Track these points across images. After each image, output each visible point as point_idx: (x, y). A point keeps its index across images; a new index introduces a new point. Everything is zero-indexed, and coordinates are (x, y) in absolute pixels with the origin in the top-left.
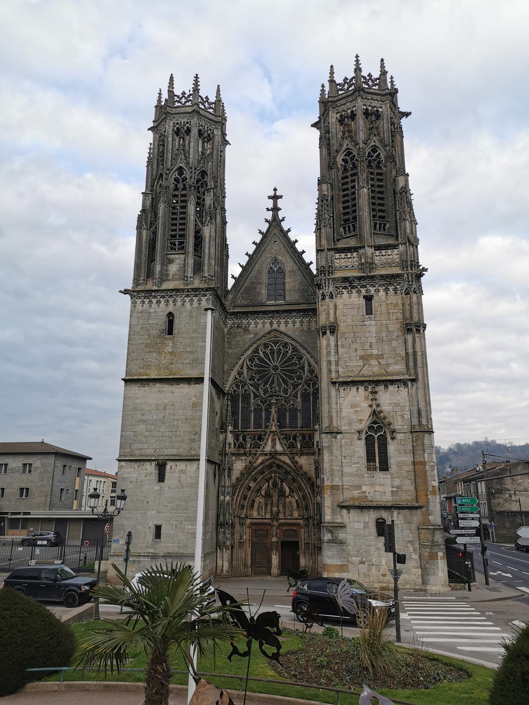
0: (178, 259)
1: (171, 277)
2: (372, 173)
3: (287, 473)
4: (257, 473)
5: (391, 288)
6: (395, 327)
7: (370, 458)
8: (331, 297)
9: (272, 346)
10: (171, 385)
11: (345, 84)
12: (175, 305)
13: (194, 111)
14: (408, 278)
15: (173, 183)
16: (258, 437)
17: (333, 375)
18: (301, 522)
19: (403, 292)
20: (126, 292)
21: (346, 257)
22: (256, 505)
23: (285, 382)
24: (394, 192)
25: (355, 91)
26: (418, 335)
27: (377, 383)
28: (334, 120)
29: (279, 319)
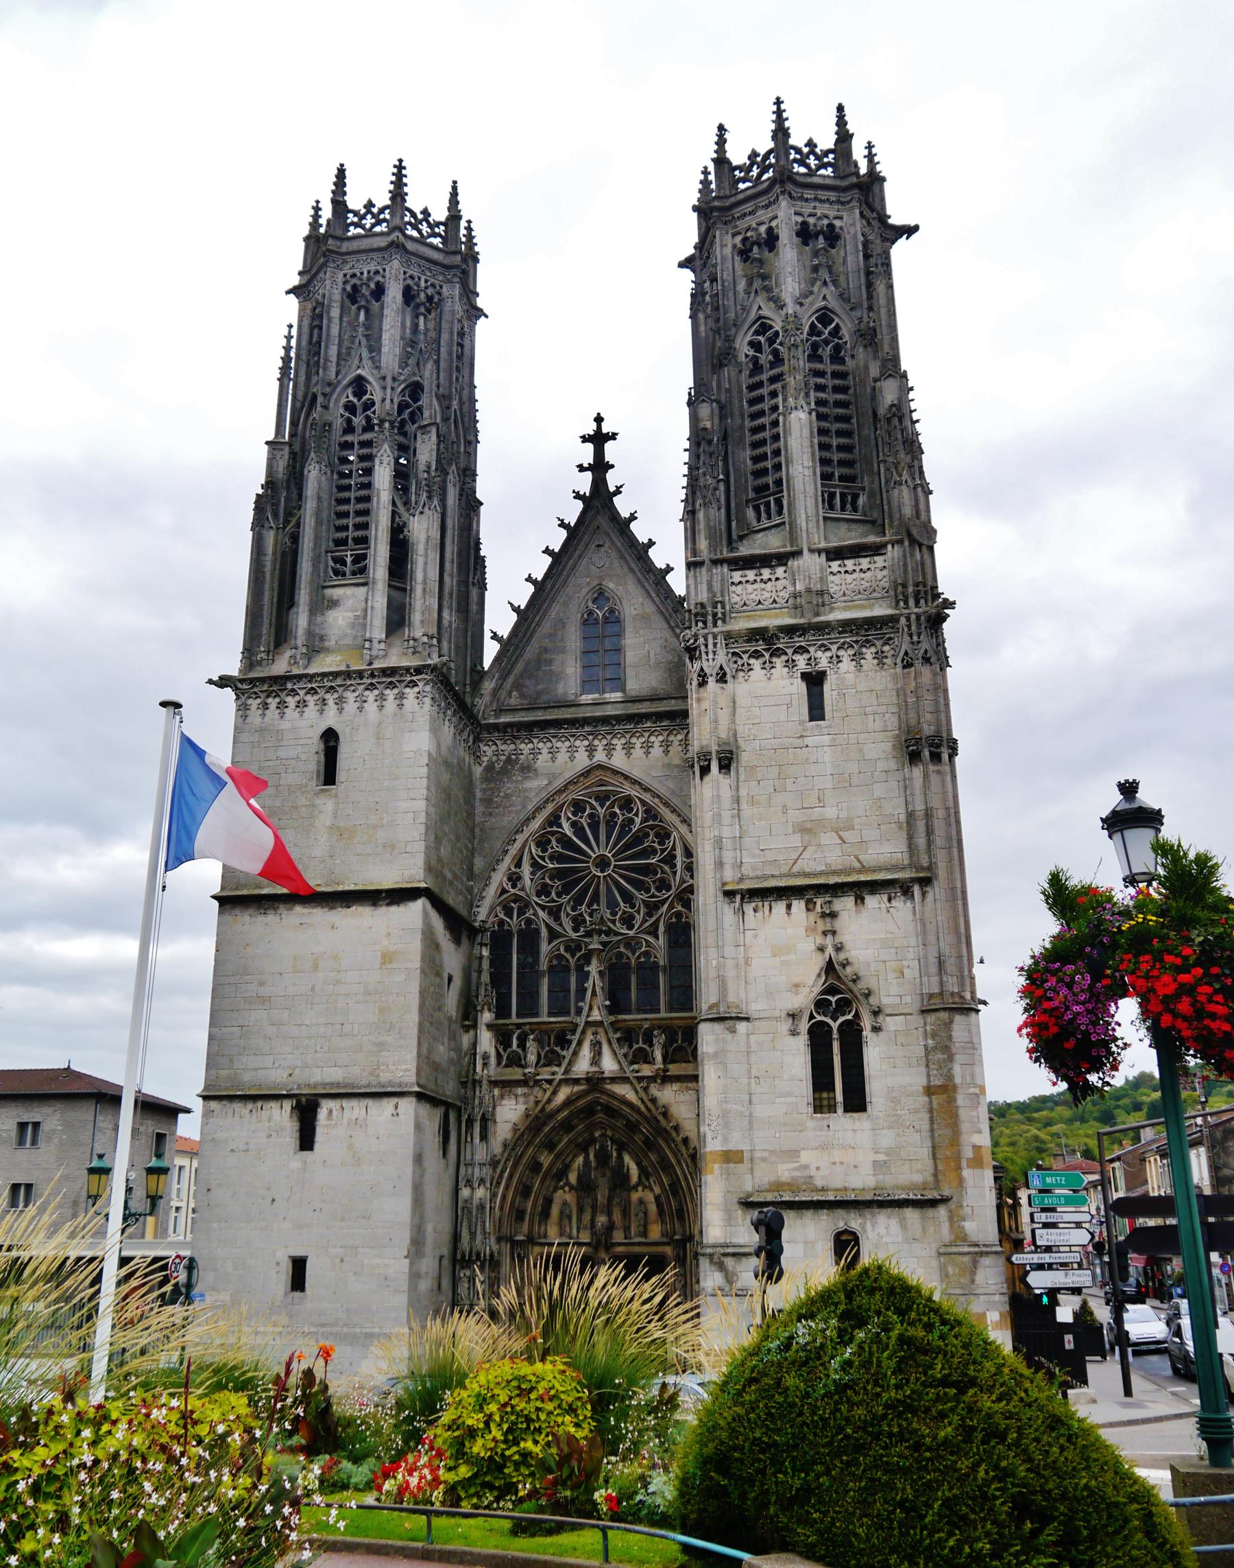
0: (350, 597)
1: (333, 643)
2: (821, 374)
3: (632, 1127)
4: (553, 1129)
5: (869, 653)
6: (879, 748)
8: (722, 678)
9: (593, 807)
10: (332, 908)
11: (752, 165)
12: (341, 710)
13: (392, 244)
14: (909, 626)
15: (342, 416)
16: (557, 1037)
18: (668, 1250)
19: (899, 661)
20: (223, 682)
21: (758, 579)
22: (555, 1211)
23: (628, 898)
24: (875, 414)
25: (773, 182)
26: (936, 768)
28: (728, 251)
29: (609, 737)
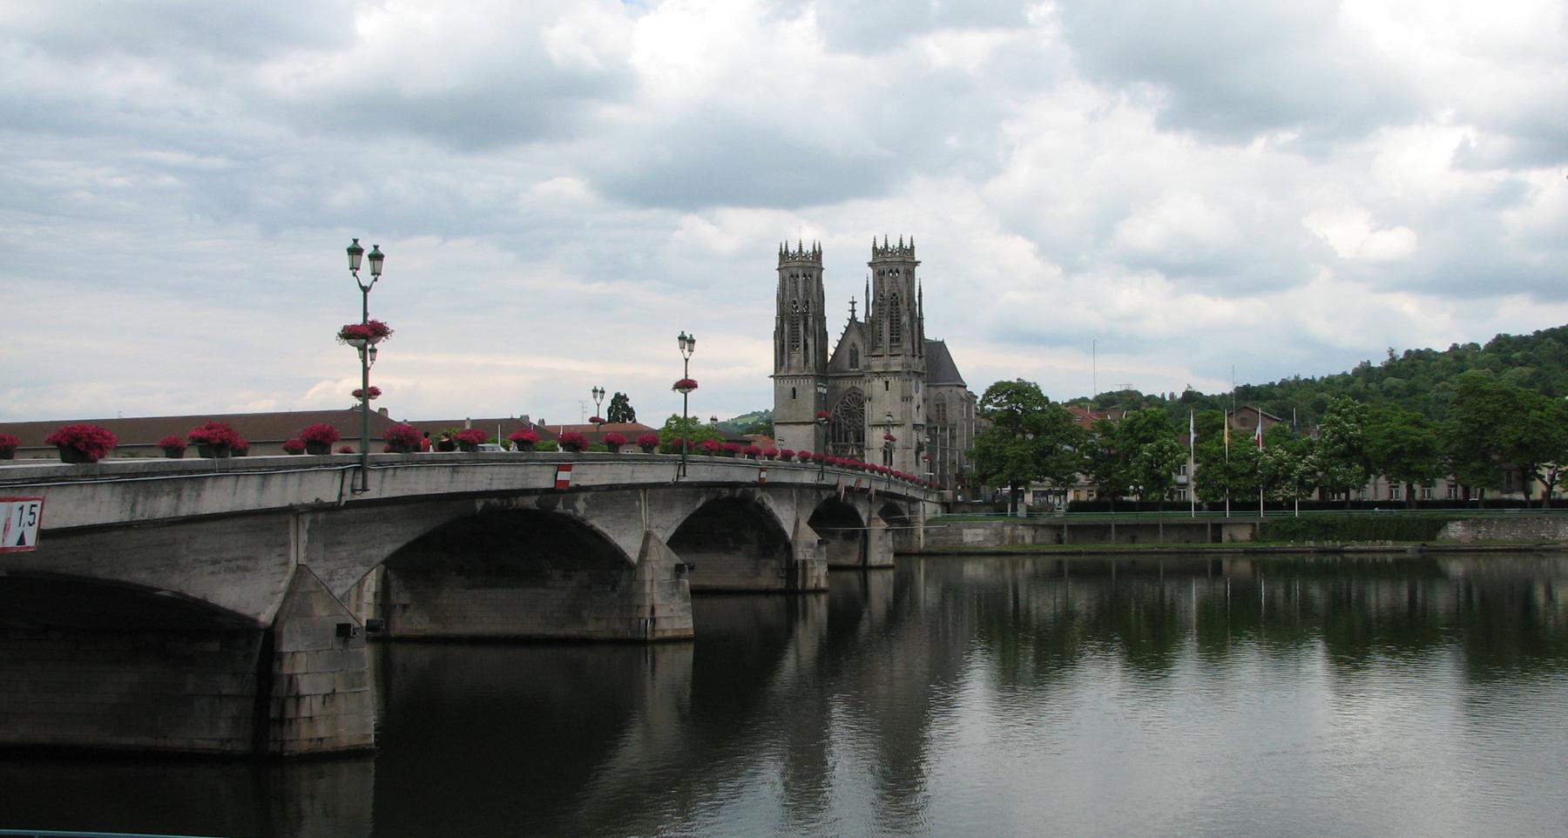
6: (898, 398)
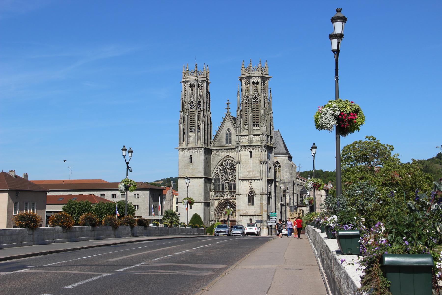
5: (257, 149)
6: (258, 162)
7: (249, 202)
17: (240, 177)
27: (252, 180)
